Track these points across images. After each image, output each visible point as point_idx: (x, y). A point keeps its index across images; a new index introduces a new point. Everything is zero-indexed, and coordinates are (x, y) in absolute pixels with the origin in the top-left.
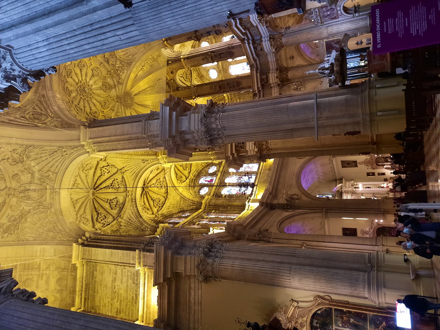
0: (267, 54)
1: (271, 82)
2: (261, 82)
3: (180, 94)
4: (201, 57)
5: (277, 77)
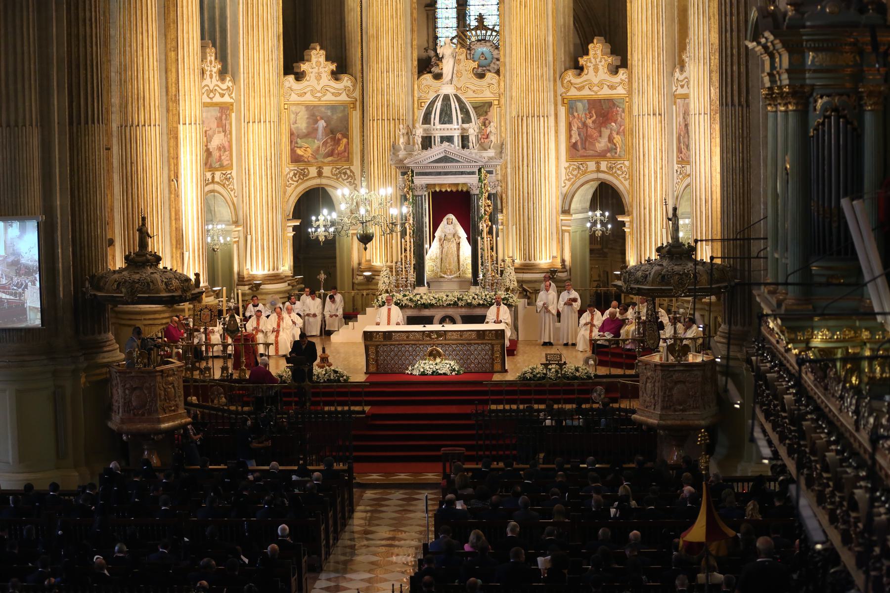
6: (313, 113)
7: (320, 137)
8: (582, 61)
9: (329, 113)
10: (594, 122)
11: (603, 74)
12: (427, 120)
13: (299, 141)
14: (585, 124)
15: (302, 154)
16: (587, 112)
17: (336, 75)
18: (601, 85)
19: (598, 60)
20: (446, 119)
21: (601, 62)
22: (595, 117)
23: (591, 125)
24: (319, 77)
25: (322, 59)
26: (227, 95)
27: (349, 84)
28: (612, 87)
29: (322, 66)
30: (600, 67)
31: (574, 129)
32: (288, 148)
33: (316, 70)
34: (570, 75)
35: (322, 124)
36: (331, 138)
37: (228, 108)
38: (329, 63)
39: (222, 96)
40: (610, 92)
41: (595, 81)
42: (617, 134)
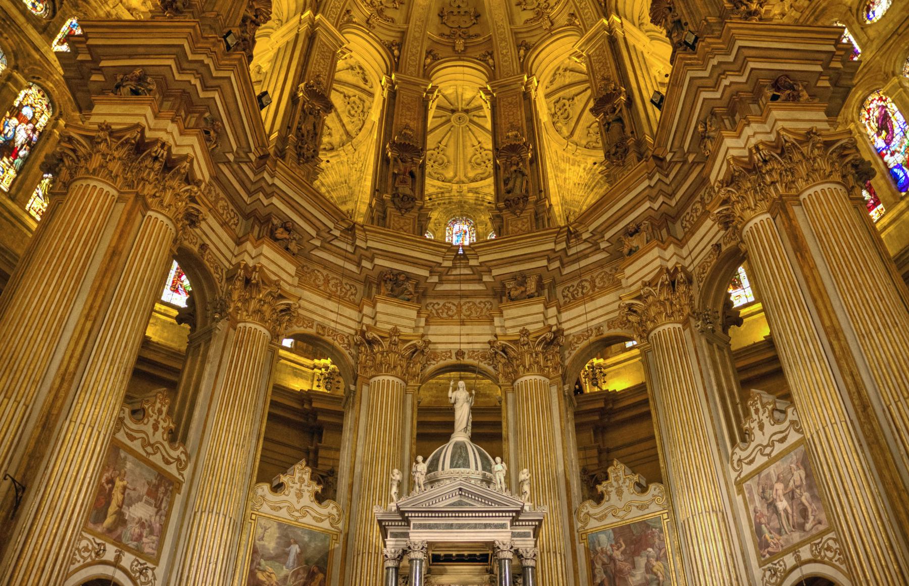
0: (617, 285)
1: (512, 312)
2: (514, 277)
3: (504, 51)
4: (613, 71)
5: (525, 333)
6: (287, 534)
7: (291, 564)
8: (600, 488)
9: (306, 539)
10: (622, 553)
11: (630, 495)
12: (433, 467)
13: (263, 562)
14: (611, 558)
15: (264, 579)
16: (613, 543)
17: (320, 498)
18: (628, 508)
19: (620, 482)
20: (460, 462)
21: (624, 482)
22: (624, 546)
23: (620, 557)
24: (299, 495)
25: (307, 477)
26: (174, 466)
27: (334, 512)
28: (641, 507)
29: (306, 483)
30: (625, 489)
31: (597, 566)
32: (247, 568)
33: (298, 486)
34: (589, 507)
35: (295, 549)
36: (304, 568)
37: (171, 484)
38: (314, 484)
39: (168, 463)
40: (641, 513)
41: (620, 505)
42: (657, 560)
